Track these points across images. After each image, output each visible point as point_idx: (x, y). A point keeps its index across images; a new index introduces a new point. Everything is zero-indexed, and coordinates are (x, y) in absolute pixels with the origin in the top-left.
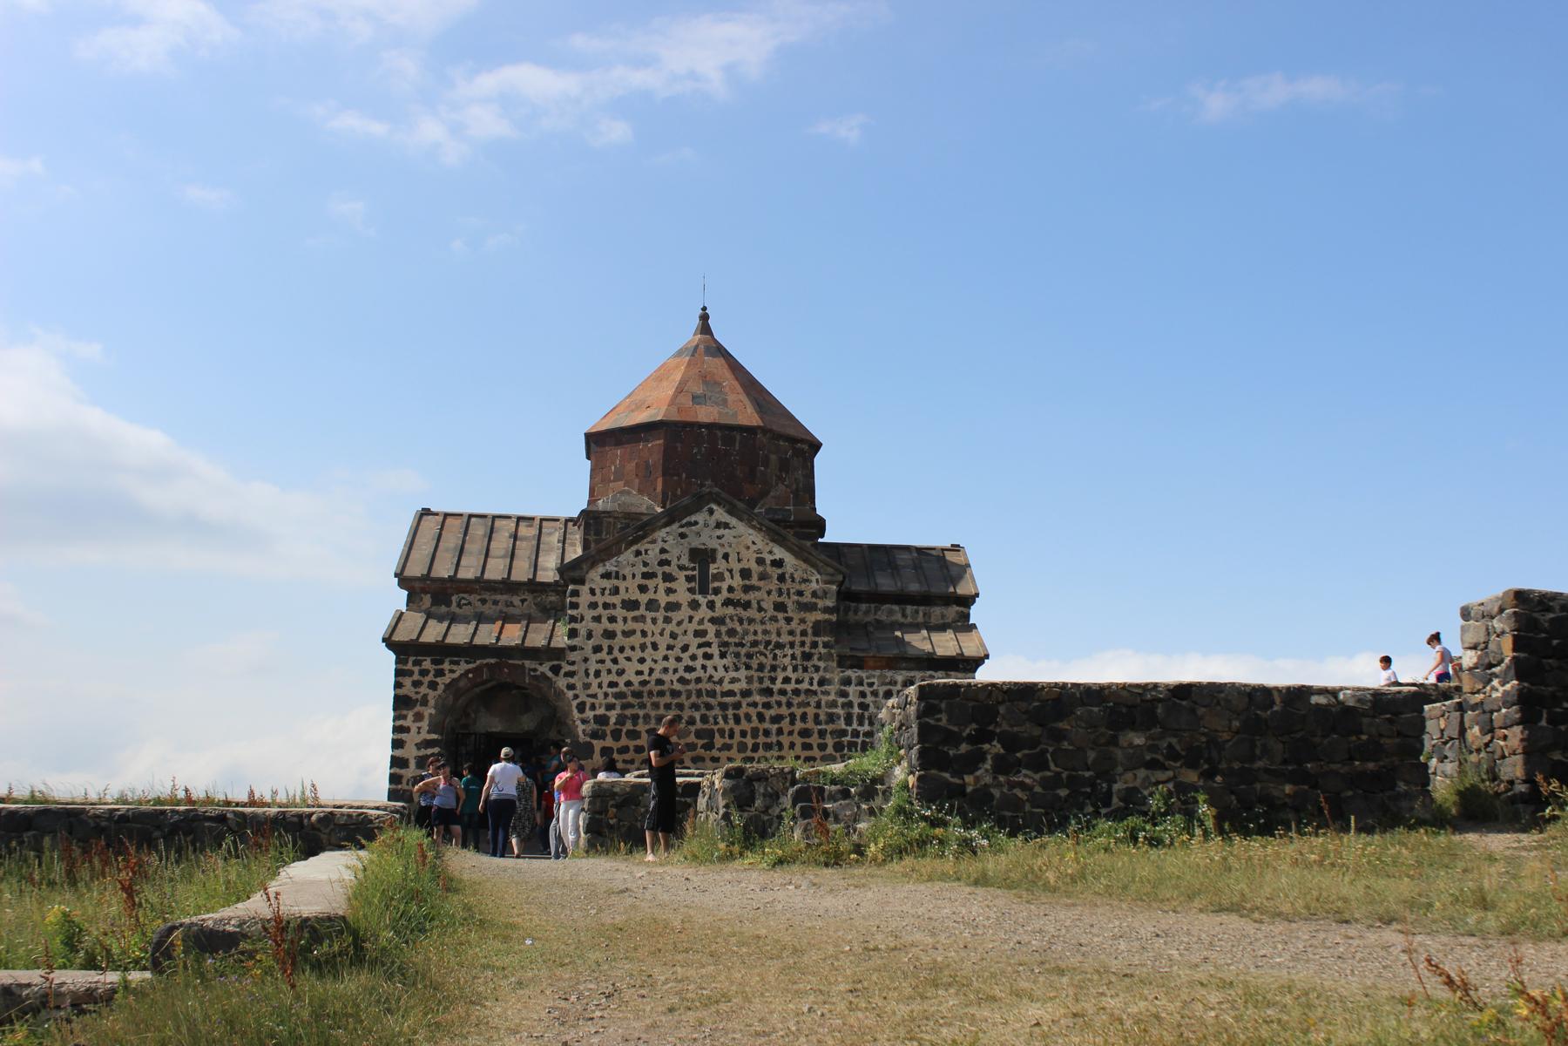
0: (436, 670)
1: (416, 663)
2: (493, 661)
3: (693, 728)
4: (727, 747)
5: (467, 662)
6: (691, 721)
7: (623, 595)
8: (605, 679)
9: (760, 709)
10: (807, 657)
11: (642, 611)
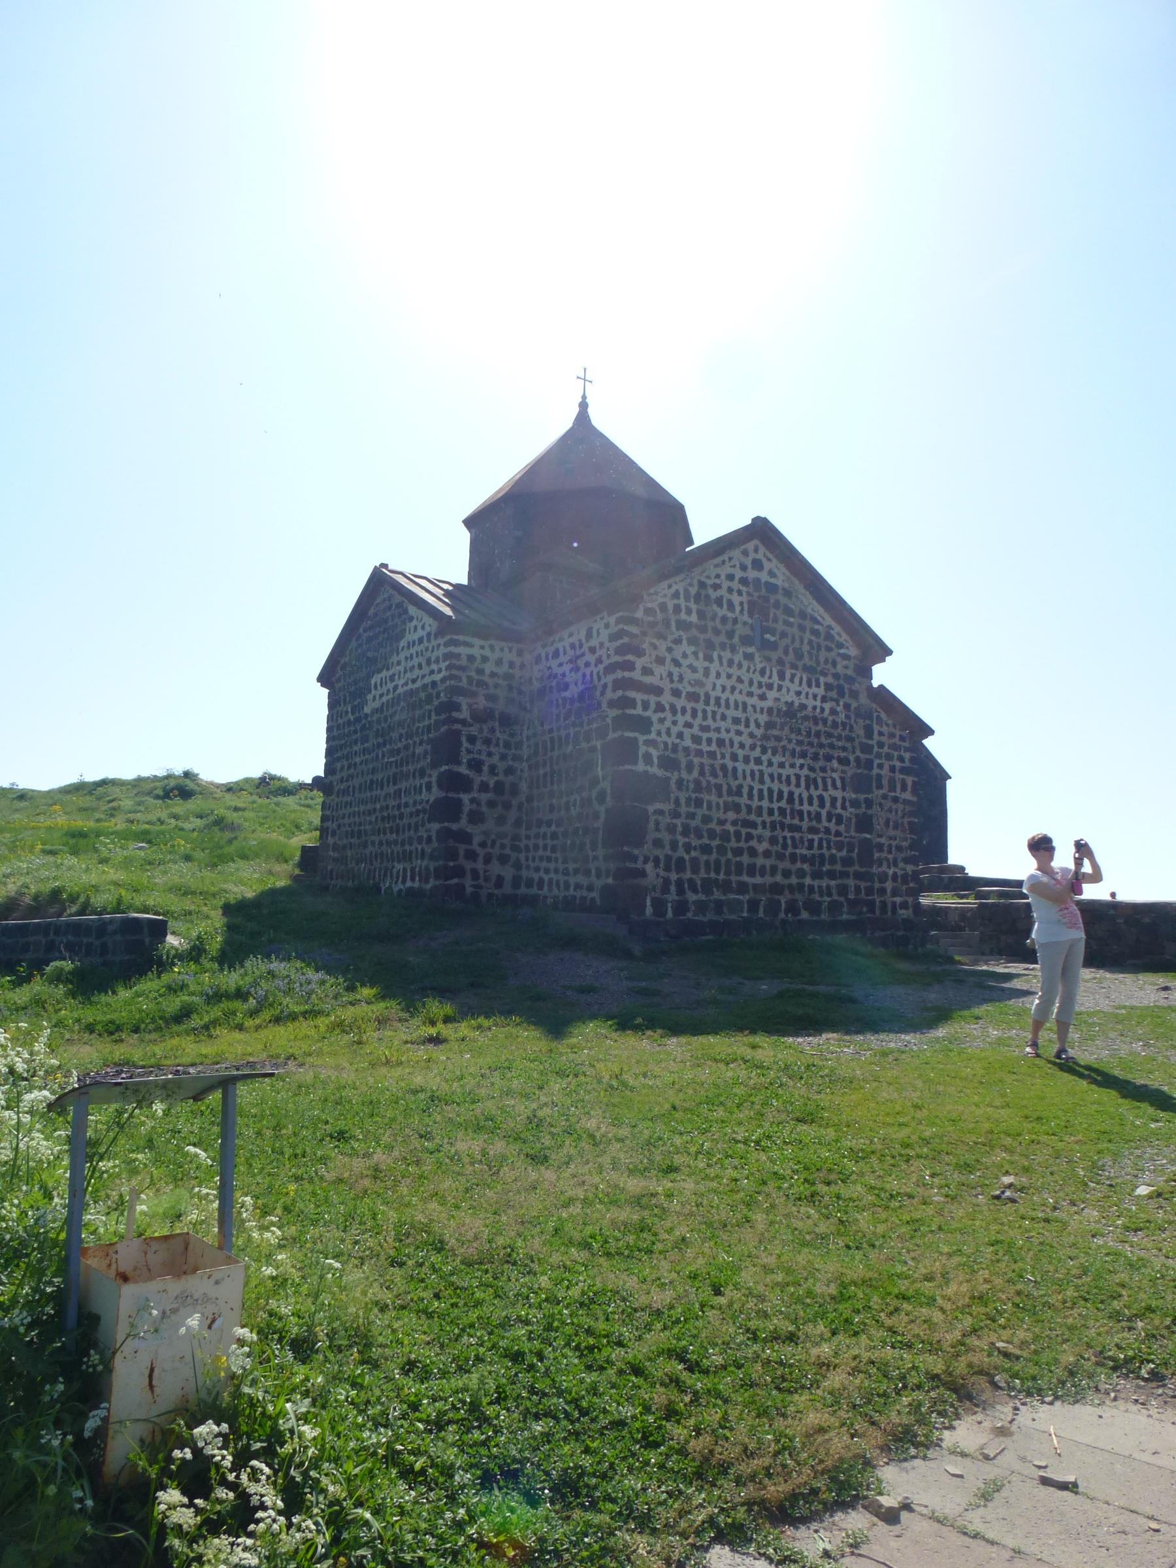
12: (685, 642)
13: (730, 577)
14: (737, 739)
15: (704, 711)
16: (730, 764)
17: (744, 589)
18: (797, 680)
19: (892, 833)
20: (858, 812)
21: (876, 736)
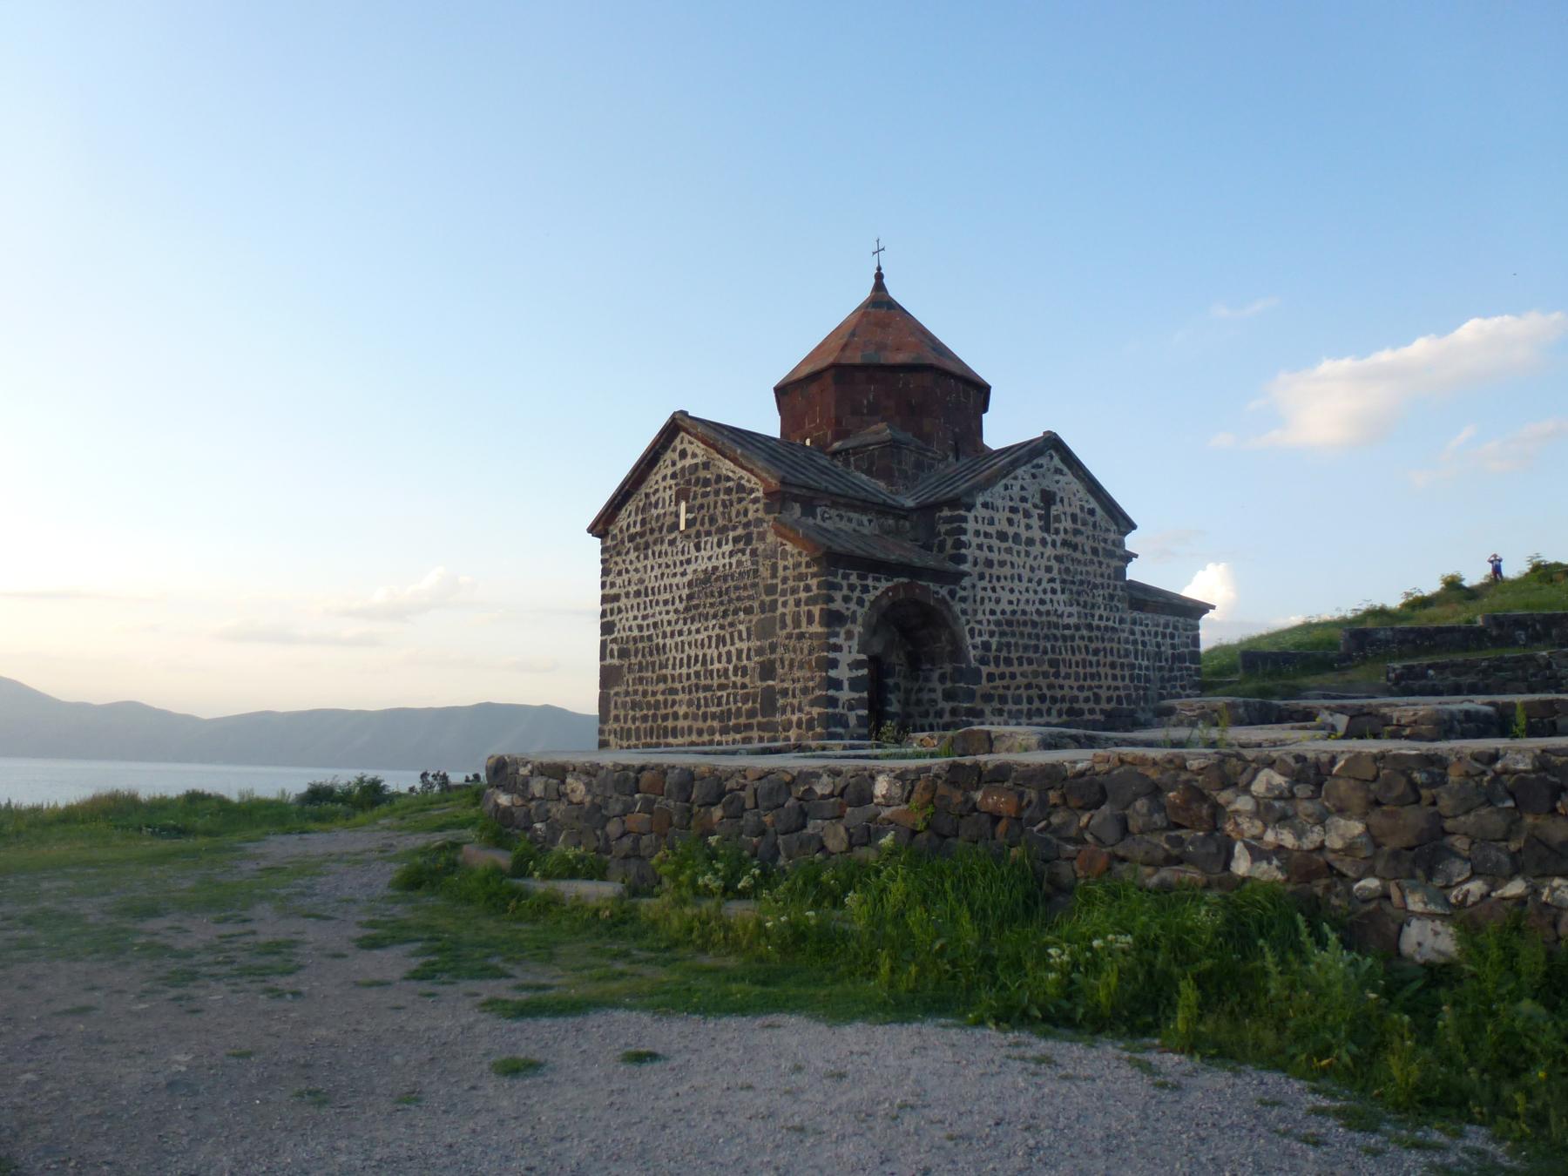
0: (862, 586)
1: (846, 577)
2: (906, 580)
3: (1046, 658)
4: (1067, 676)
5: (887, 580)
6: (1045, 652)
7: (997, 527)
8: (988, 606)
9: (1086, 642)
10: (1112, 597)
11: (1010, 543)
12: (632, 551)
13: (664, 478)
14: (666, 618)
15: (645, 602)
16: (661, 641)
17: (673, 482)
18: (709, 546)
19: (798, 674)
20: (762, 659)
21: (781, 573)
